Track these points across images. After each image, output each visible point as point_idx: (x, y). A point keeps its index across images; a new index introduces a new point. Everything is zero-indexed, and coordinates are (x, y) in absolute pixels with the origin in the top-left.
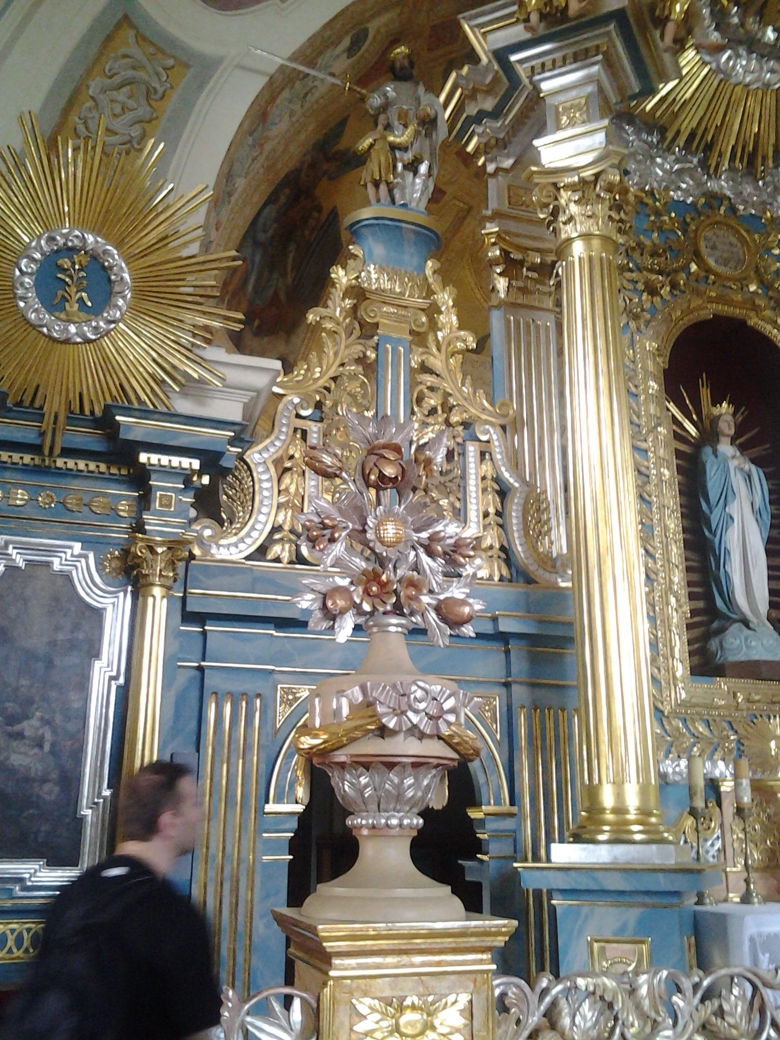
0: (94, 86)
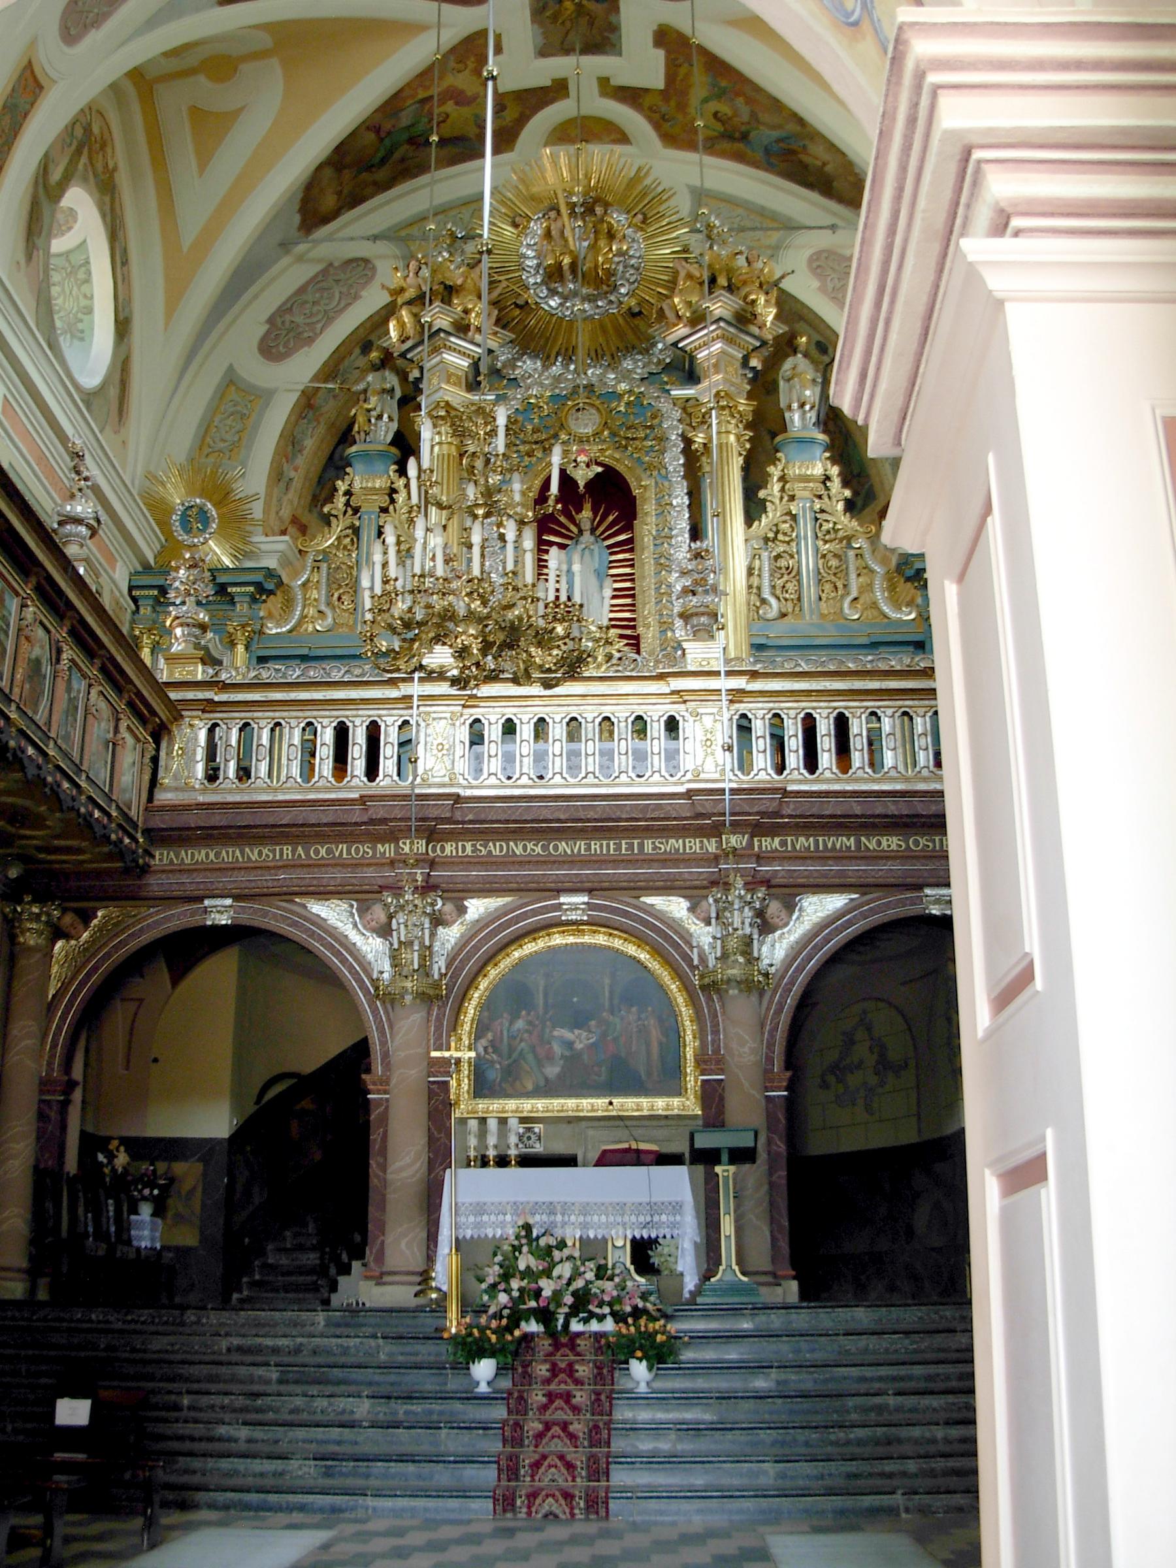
0: (217, 420)
